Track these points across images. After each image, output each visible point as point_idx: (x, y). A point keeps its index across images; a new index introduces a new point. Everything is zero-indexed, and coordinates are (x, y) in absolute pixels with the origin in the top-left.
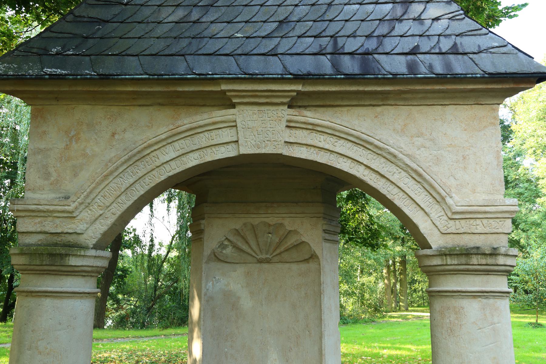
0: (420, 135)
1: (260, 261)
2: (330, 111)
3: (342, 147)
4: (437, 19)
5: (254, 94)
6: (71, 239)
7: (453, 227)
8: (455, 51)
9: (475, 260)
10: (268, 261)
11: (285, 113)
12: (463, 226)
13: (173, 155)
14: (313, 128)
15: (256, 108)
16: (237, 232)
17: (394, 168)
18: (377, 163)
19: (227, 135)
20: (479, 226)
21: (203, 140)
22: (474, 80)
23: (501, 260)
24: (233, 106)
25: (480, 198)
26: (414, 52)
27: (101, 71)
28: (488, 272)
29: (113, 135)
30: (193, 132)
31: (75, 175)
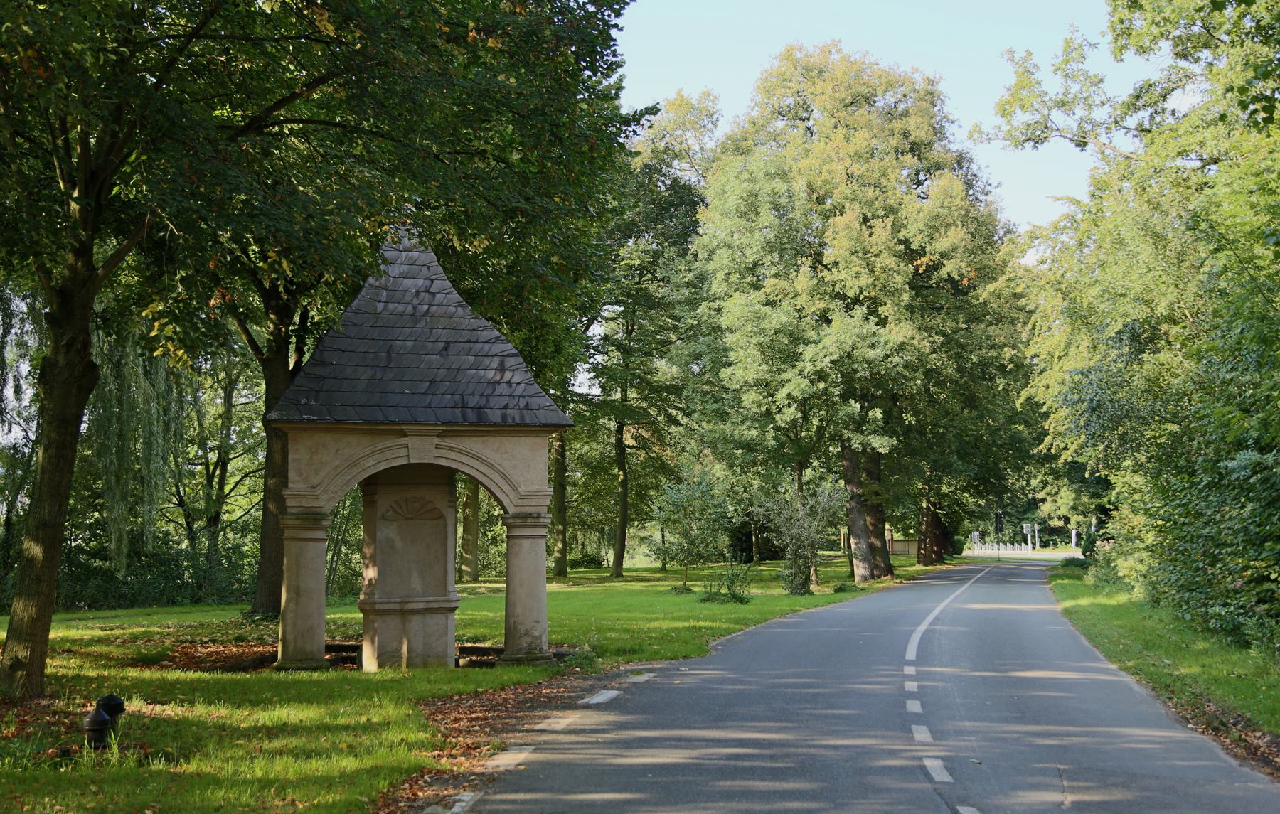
0: (506, 453)
1: (407, 519)
2: (458, 439)
3: (464, 459)
4: (519, 383)
5: (419, 431)
6: (317, 510)
7: (520, 502)
8: (527, 407)
9: (529, 520)
10: (412, 519)
11: (436, 440)
12: (526, 502)
13: (372, 463)
14: (450, 449)
15: (419, 438)
16: (396, 502)
17: (492, 471)
18: (483, 468)
19: (403, 452)
20: (534, 502)
21: (389, 454)
22: (536, 426)
23: (542, 520)
24: (406, 436)
25: (535, 487)
26: (506, 407)
27: (336, 418)
28: (535, 526)
29: (337, 451)
30: (384, 450)
31: (317, 474)
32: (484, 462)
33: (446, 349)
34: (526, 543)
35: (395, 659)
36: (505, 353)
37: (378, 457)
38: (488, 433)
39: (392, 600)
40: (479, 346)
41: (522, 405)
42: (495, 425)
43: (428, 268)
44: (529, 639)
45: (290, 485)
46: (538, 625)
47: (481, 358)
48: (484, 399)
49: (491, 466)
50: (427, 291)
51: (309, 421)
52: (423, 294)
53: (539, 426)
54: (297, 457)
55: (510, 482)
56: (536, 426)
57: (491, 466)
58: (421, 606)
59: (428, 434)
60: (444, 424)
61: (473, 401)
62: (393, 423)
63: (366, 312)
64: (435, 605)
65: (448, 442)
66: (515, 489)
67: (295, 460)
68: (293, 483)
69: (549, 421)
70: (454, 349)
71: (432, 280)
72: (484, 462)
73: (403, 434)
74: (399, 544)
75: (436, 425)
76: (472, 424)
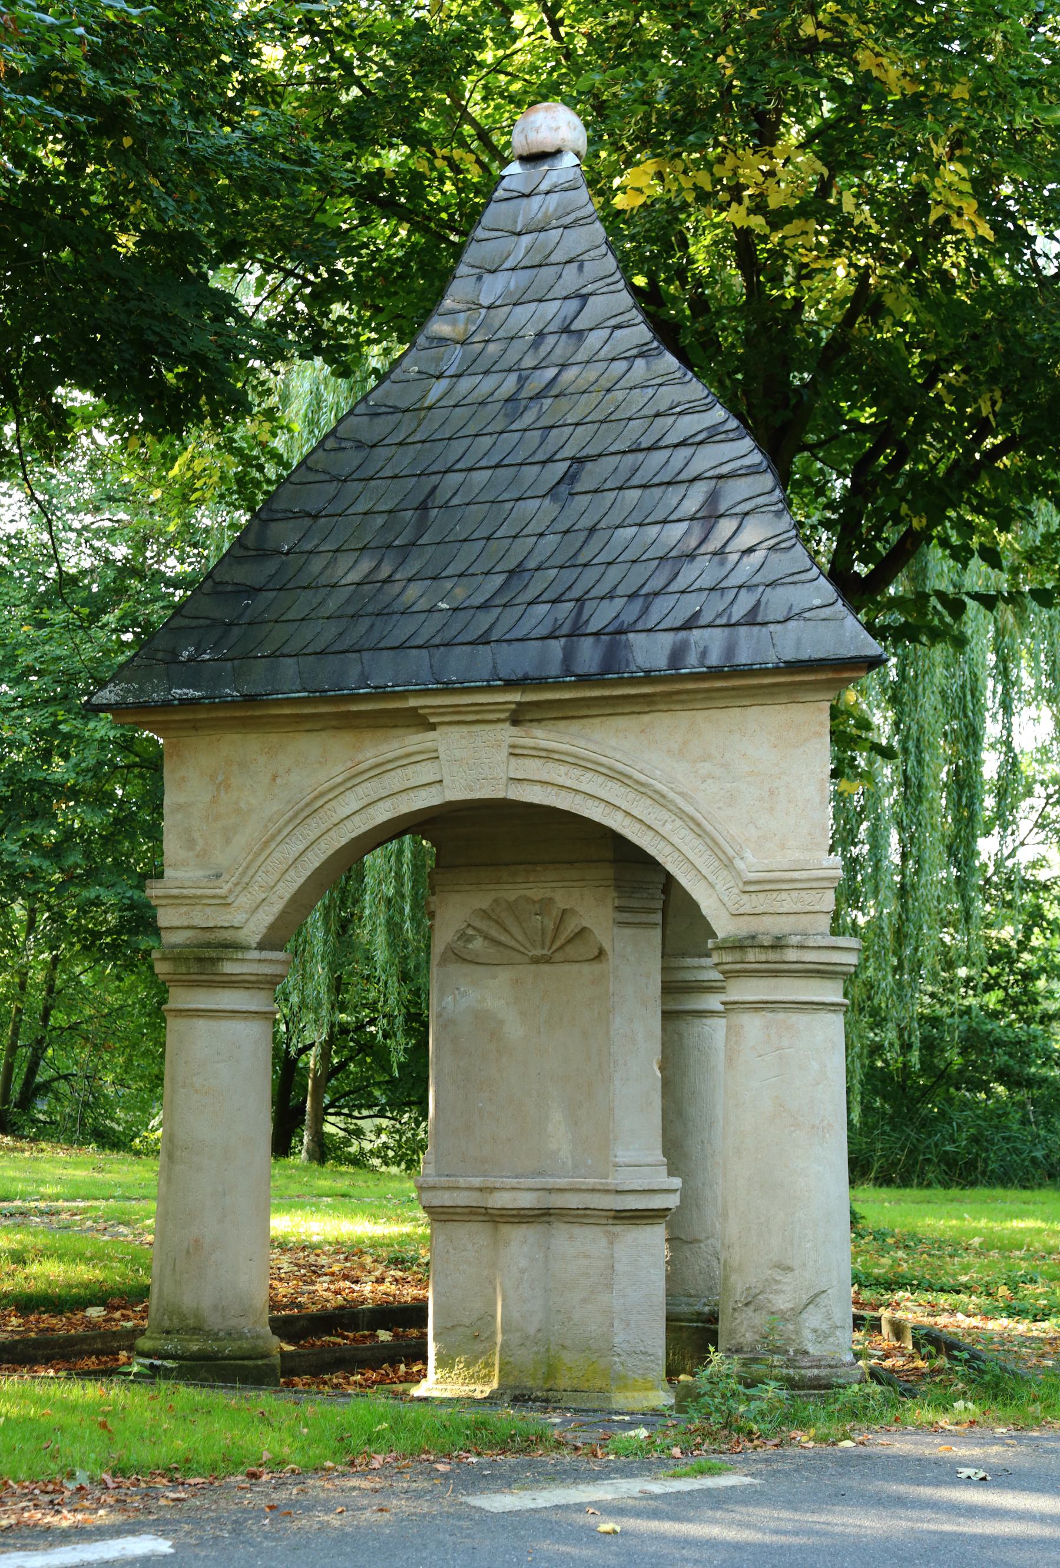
0: (706, 758)
1: (536, 961)
2: (575, 726)
3: (590, 783)
4: (750, 550)
5: (456, 709)
6: (227, 935)
7: (748, 904)
8: (752, 619)
9: (752, 955)
10: (548, 960)
11: (507, 734)
12: (760, 902)
13: (355, 806)
14: (548, 755)
15: (465, 729)
16: (485, 914)
17: (665, 815)
18: (641, 808)
19: (425, 773)
20: (787, 902)
21: (395, 780)
22: (765, 672)
23: (792, 955)
24: (433, 727)
25: (793, 855)
26: (688, 625)
27: (246, 690)
28: (776, 973)
29: (274, 778)
30: (381, 769)
31: (228, 842)
32: (641, 789)
33: (569, 478)
34: (753, 1024)
35: (480, 1347)
36: (724, 470)
37: (368, 790)
38: (648, 703)
39: (462, 1182)
40: (658, 458)
41: (738, 612)
42: (649, 677)
43: (581, 268)
44: (760, 1320)
45: (168, 872)
46: (788, 1278)
47: (657, 492)
48: (638, 604)
49: (660, 799)
50: (566, 330)
51: (187, 703)
52: (551, 340)
53: (776, 670)
54: (182, 799)
55: (713, 845)
56: (765, 672)
57: (660, 799)
58: (526, 1200)
59: (478, 718)
60: (510, 684)
61: (601, 616)
62: (381, 693)
63: (396, 410)
64: (573, 1201)
65: (541, 736)
66: (728, 864)
67: (179, 807)
68: (174, 866)
69: (807, 653)
70: (591, 476)
71: (584, 298)
72: (641, 789)
73: (421, 722)
74: (514, 1030)
75: (489, 689)
76: (584, 680)
